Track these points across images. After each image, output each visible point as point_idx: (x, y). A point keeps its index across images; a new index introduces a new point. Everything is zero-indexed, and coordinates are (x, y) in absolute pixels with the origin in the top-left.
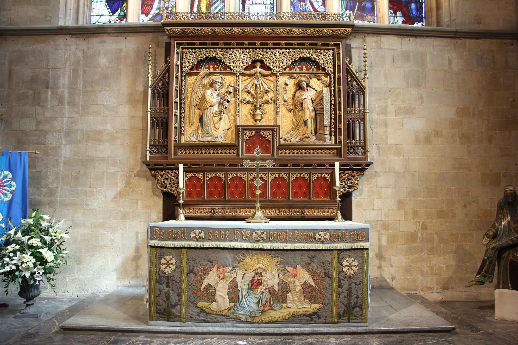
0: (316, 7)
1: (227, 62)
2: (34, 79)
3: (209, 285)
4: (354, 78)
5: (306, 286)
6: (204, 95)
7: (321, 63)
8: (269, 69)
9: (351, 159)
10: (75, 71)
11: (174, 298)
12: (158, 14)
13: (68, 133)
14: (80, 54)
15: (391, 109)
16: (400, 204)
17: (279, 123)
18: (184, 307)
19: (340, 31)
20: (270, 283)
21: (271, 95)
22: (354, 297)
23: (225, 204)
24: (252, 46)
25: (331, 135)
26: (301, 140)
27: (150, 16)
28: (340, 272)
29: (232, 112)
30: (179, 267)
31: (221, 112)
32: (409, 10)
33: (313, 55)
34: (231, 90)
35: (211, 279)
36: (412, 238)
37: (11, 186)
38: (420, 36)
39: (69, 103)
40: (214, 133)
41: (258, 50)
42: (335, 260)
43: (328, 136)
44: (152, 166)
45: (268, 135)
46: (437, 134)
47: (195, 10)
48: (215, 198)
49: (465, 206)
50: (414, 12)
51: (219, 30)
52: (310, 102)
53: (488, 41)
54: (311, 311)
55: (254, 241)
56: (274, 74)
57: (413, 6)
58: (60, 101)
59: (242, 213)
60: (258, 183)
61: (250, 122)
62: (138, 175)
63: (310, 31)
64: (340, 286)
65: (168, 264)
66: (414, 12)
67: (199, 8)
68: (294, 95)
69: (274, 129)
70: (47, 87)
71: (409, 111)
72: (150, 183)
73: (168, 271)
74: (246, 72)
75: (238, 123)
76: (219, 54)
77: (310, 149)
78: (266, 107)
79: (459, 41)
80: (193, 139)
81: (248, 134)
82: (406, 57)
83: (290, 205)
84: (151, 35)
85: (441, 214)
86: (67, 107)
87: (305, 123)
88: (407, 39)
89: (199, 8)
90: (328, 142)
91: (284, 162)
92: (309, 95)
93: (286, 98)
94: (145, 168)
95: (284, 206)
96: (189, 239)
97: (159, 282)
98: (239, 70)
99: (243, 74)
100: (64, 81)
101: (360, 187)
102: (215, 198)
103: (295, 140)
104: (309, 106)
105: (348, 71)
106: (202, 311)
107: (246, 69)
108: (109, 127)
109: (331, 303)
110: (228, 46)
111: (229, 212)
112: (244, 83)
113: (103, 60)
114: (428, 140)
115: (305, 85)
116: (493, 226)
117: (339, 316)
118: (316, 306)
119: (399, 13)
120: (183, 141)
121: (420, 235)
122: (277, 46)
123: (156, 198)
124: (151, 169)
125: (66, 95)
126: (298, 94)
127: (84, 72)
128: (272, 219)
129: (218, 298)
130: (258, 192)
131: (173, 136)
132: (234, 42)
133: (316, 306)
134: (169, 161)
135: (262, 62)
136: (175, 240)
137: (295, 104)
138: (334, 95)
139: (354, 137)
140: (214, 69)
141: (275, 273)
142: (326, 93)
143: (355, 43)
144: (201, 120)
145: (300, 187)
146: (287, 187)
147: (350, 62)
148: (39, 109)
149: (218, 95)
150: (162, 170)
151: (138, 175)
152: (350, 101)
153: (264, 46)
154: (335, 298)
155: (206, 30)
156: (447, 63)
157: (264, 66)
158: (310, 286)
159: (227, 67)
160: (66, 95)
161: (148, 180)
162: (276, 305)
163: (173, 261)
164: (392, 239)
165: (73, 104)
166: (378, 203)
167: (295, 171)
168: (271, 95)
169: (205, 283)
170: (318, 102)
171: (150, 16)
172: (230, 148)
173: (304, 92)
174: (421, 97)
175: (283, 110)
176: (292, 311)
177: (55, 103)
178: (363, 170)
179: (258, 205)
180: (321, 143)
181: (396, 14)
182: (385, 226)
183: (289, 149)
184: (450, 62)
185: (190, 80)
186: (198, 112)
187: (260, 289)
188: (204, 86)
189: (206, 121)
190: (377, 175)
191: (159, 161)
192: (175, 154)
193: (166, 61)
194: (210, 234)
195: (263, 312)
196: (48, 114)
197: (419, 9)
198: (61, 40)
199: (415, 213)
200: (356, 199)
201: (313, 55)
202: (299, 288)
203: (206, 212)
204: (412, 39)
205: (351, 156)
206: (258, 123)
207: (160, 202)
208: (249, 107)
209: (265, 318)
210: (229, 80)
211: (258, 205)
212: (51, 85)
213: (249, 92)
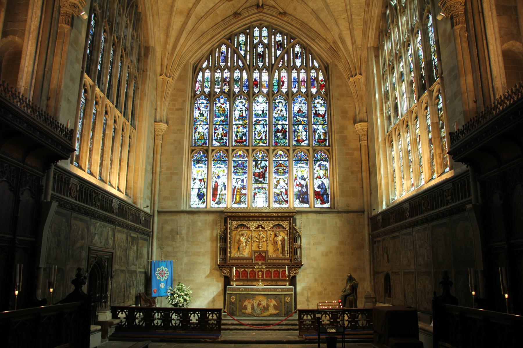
0: (284, 198)
1: (248, 226)
2: (172, 231)
3: (245, 305)
4: (297, 232)
5: (274, 305)
6: (240, 239)
7: (284, 226)
8: (264, 228)
9: (295, 263)
10: (188, 228)
11: (234, 309)
12: (219, 201)
13: (186, 252)
14: (190, 221)
15: (312, 243)
16: (316, 280)
17: (268, 250)
18: (238, 312)
19: (291, 214)
20: (264, 304)
21: (265, 239)
22: (289, 308)
23: (248, 280)
24: (258, 220)
25: (288, 254)
26: (277, 256)
27: (216, 202)
28: (285, 301)
29: (250, 245)
30: (236, 299)
31: (246, 245)
32: (323, 198)
33: (281, 223)
34: (250, 237)
35: (246, 303)
36: (320, 293)
37: (167, 273)
38: (324, 213)
39: (186, 241)
40: (244, 253)
41: (260, 222)
42: (283, 297)
43: (287, 254)
44: (221, 266)
45: (264, 254)
46: (331, 252)
47: (234, 200)
48: (244, 278)
49: (342, 281)
50: (325, 199)
51: (245, 214)
52: (280, 241)
53: (352, 214)
54: (276, 313)
55: (259, 291)
56: (265, 231)
57: (325, 196)
58: (183, 240)
59: (254, 284)
60: (260, 273)
61: (257, 250)
62: (214, 269)
63: (280, 214)
64: (285, 305)
65: (233, 299)
66: (325, 199)
67: (236, 199)
68: (274, 239)
69: (266, 252)
70: (177, 234)
71: (319, 243)
72: (219, 272)
73: (233, 301)
74: (256, 230)
75: (253, 250)
76: (245, 223)
77: (280, 259)
78: (263, 243)
79: (340, 214)
80: (236, 256)
81: (257, 254)
82: (318, 222)
83: (272, 281)
84: (218, 214)
85: (332, 284)
86: (185, 242)
87: (278, 249)
88: (319, 215)
89: (236, 199)
90: (287, 256)
91: (270, 264)
92: (280, 238)
93: (271, 239)
94: (217, 266)
95: (270, 281)
96: (239, 291)
97: (230, 304)
98: (254, 229)
99: (254, 231)
100: (184, 232)
101: (299, 273)
102: (244, 278)
103: (274, 256)
104: (280, 242)
105: (294, 229)
106: (243, 313)
107: (256, 228)
108: (202, 250)
109: (282, 311)
110: (249, 220)
111: (250, 283)
112: (255, 234)
113: (200, 224)
114: (327, 255)
115: (278, 235)
116: (345, 288)
117: (285, 315)
118: (277, 311)
119: (319, 200)
120: (232, 257)
121: (324, 292)
122: (267, 220)
123: (221, 278)
124: (220, 267)
125: (185, 237)
126: (275, 238)
127: (192, 228)
128: (265, 285)
129: (248, 309)
130: (260, 276)
131: (229, 255)
132: (251, 218)
133: (277, 311)
134: (227, 264)
135: (261, 226)
136: (236, 291)
137: (274, 242)
138: (290, 238)
139: (297, 254)
140: (243, 228)
141: (265, 301)
142: (286, 238)
143: (298, 217)
144: (239, 248)
145: (276, 274)
146: (271, 274)
147: (296, 225)
148: (174, 243)
149: (245, 239)
150: (224, 267)
151: (214, 269)
152: (295, 241)
153: (263, 220)
154: (283, 309)
155: (240, 214)
156: (335, 224)
157: (262, 228)
158: (276, 305)
159: (248, 228)
160: (185, 237)
161: (218, 271)
162: (265, 311)
163: (235, 298)
164: (313, 294)
165: (188, 241)
166: (307, 280)
167: (274, 268)
168: (265, 239)
169: (244, 304)
170: (283, 240)
171: (216, 202)
172: (250, 259)
173: (278, 238)
174: (324, 238)
175: (270, 245)
176: (270, 313)
177: (181, 240)
178: (300, 267)
179: (260, 281)
180: (284, 257)
181: (317, 200)
182: (310, 289)
183: (272, 259)
184: (336, 223)
185: (234, 233)
186: (237, 245)
187: (261, 306)
188: (240, 235)
189: (241, 249)
190: (306, 269)
191: (223, 264)
192: (229, 261)
193: (225, 225)
194: (245, 290)
195: (262, 313)
196: (178, 245)
197: (328, 197)
198: (182, 216)
199: (322, 284)
200: (298, 278)
201: (281, 223)
202: (272, 306)
203: (242, 283)
204: (321, 214)
205: (296, 262)
206: (261, 250)
207: (223, 279)
208: (257, 243)
209: (262, 315)
210: (249, 233)
211: (260, 281)
212: (179, 233)
213: (257, 238)
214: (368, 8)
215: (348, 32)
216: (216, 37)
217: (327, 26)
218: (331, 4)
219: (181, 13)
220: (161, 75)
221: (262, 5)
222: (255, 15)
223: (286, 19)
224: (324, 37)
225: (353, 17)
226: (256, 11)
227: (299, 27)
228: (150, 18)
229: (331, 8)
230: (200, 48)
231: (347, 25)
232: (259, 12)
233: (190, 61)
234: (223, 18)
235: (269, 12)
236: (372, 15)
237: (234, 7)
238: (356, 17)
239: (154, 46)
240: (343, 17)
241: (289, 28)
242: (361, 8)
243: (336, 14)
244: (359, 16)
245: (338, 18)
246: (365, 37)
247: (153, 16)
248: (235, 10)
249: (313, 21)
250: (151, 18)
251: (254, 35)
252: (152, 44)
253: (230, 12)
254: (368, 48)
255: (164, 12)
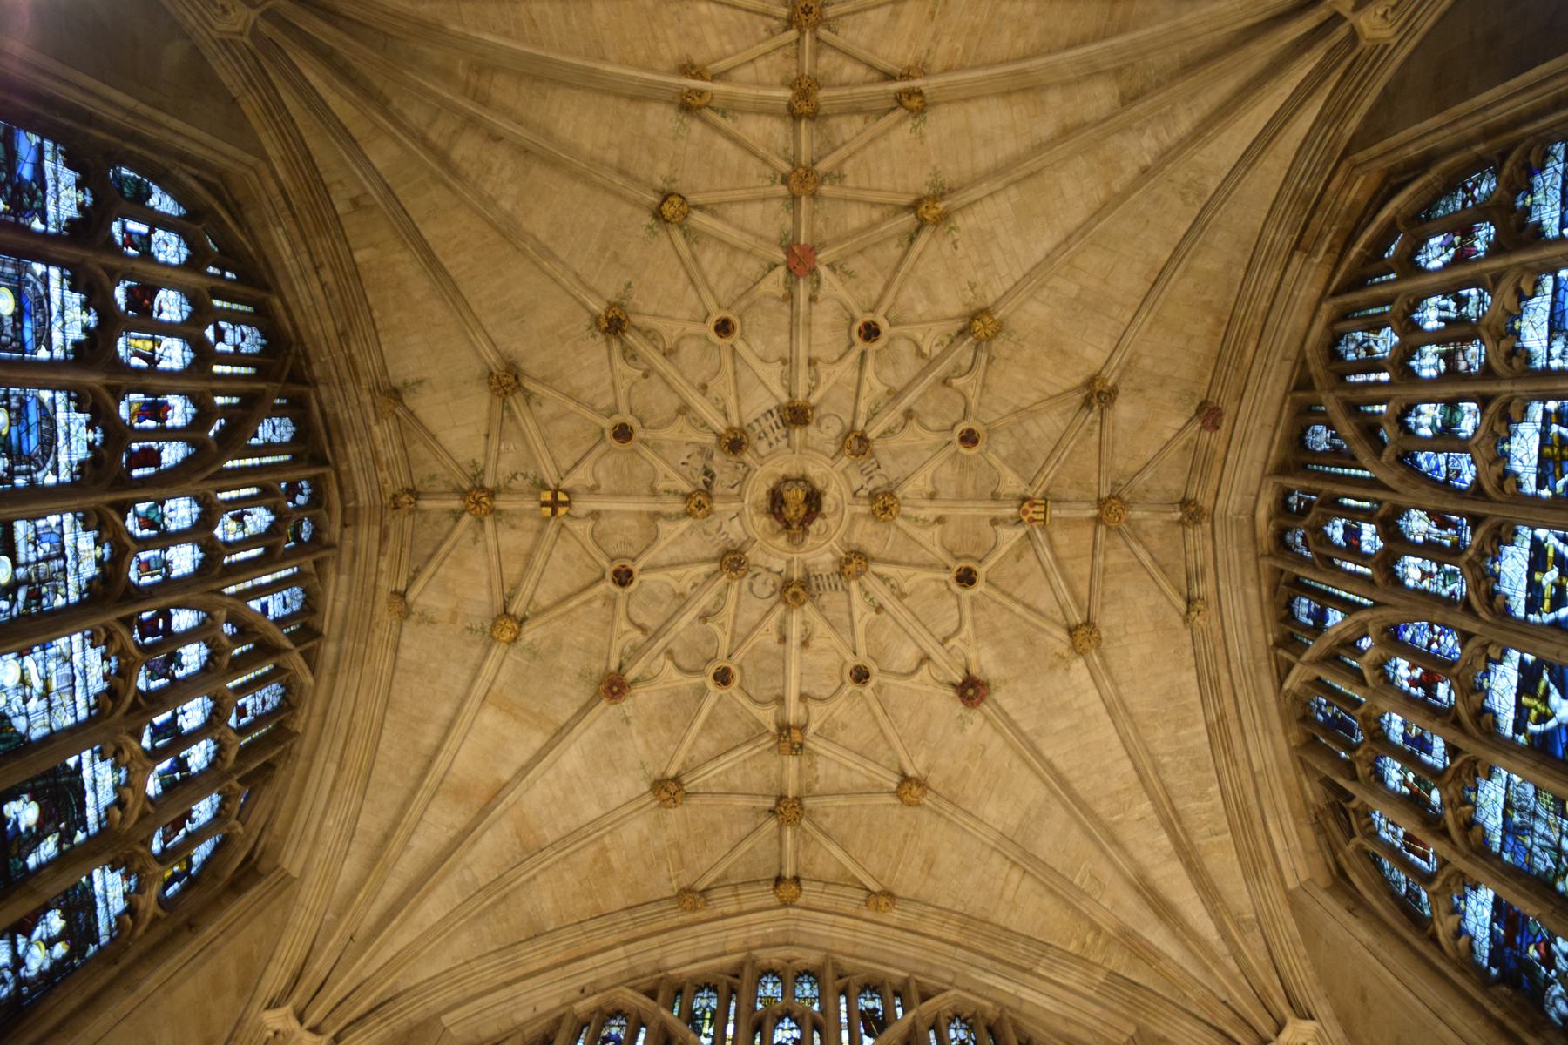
214: (1228, 748)
215: (1177, 867)
216: (588, 963)
217: (1077, 881)
218: (1076, 774)
219: (460, 793)
220: (273, 1005)
221: (796, 879)
222: (765, 914)
223: (894, 916)
224: (1072, 948)
225: (1180, 805)
226: (772, 900)
227: (954, 938)
228: (325, 769)
229: (1076, 786)
230: (507, 984)
231: (1164, 839)
232: (785, 904)
233: (446, 1019)
234: (631, 902)
235: (825, 902)
236: (1256, 765)
237: (682, 863)
238: (1193, 805)
239: (295, 873)
240: (1137, 816)
241: (911, 952)
242: (1198, 768)
243: (1102, 808)
244: (1200, 798)
245: (1118, 823)
246: (1254, 865)
247: (341, 766)
248: (686, 879)
249: (1009, 894)
250: (332, 768)
251: (761, 993)
252: (292, 861)
253: (665, 882)
254: (1292, 899)
255: (392, 777)
